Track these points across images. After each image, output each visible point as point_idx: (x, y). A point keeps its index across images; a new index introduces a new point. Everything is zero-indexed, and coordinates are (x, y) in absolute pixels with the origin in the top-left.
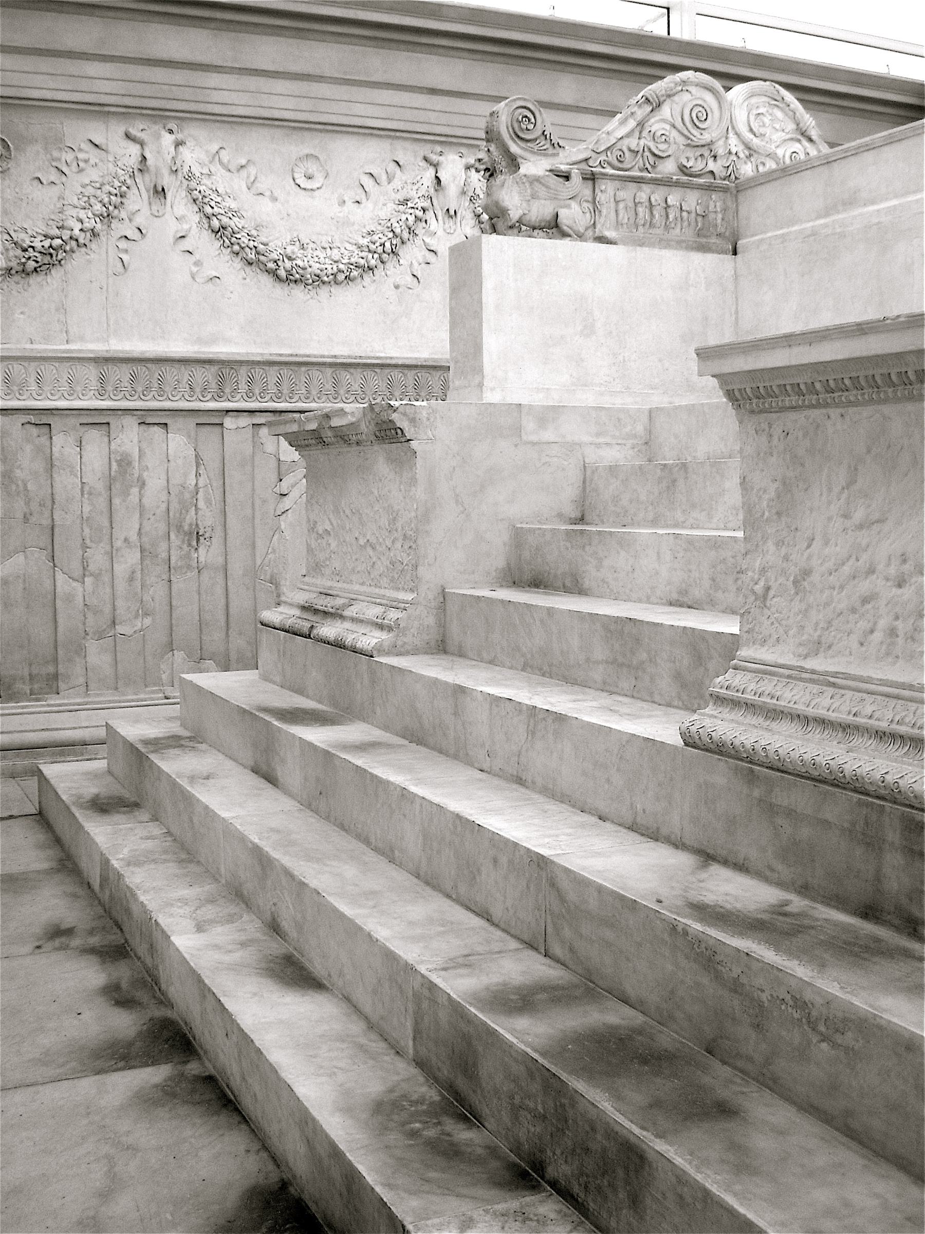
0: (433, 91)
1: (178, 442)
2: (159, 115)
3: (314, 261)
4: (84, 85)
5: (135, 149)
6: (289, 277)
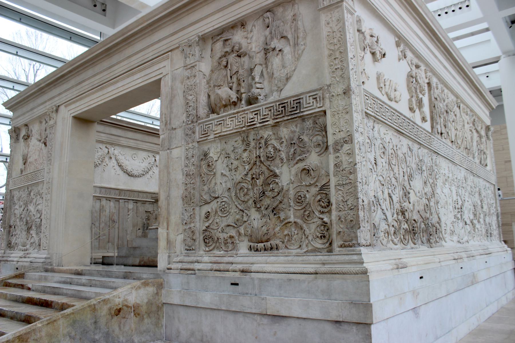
0: (156, 144)
1: (112, 204)
2: (112, 144)
3: (135, 173)
4: (100, 137)
5: (107, 150)
6: (130, 175)
